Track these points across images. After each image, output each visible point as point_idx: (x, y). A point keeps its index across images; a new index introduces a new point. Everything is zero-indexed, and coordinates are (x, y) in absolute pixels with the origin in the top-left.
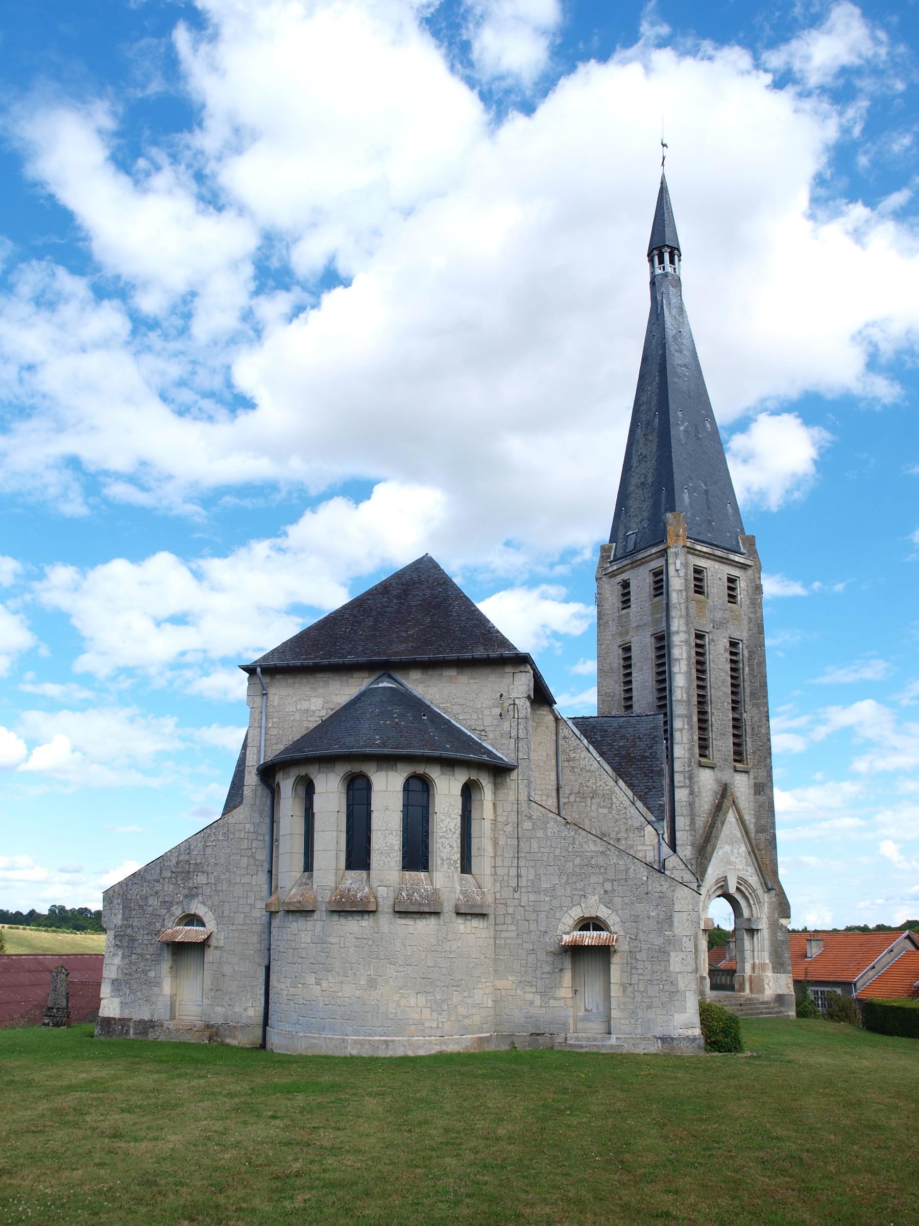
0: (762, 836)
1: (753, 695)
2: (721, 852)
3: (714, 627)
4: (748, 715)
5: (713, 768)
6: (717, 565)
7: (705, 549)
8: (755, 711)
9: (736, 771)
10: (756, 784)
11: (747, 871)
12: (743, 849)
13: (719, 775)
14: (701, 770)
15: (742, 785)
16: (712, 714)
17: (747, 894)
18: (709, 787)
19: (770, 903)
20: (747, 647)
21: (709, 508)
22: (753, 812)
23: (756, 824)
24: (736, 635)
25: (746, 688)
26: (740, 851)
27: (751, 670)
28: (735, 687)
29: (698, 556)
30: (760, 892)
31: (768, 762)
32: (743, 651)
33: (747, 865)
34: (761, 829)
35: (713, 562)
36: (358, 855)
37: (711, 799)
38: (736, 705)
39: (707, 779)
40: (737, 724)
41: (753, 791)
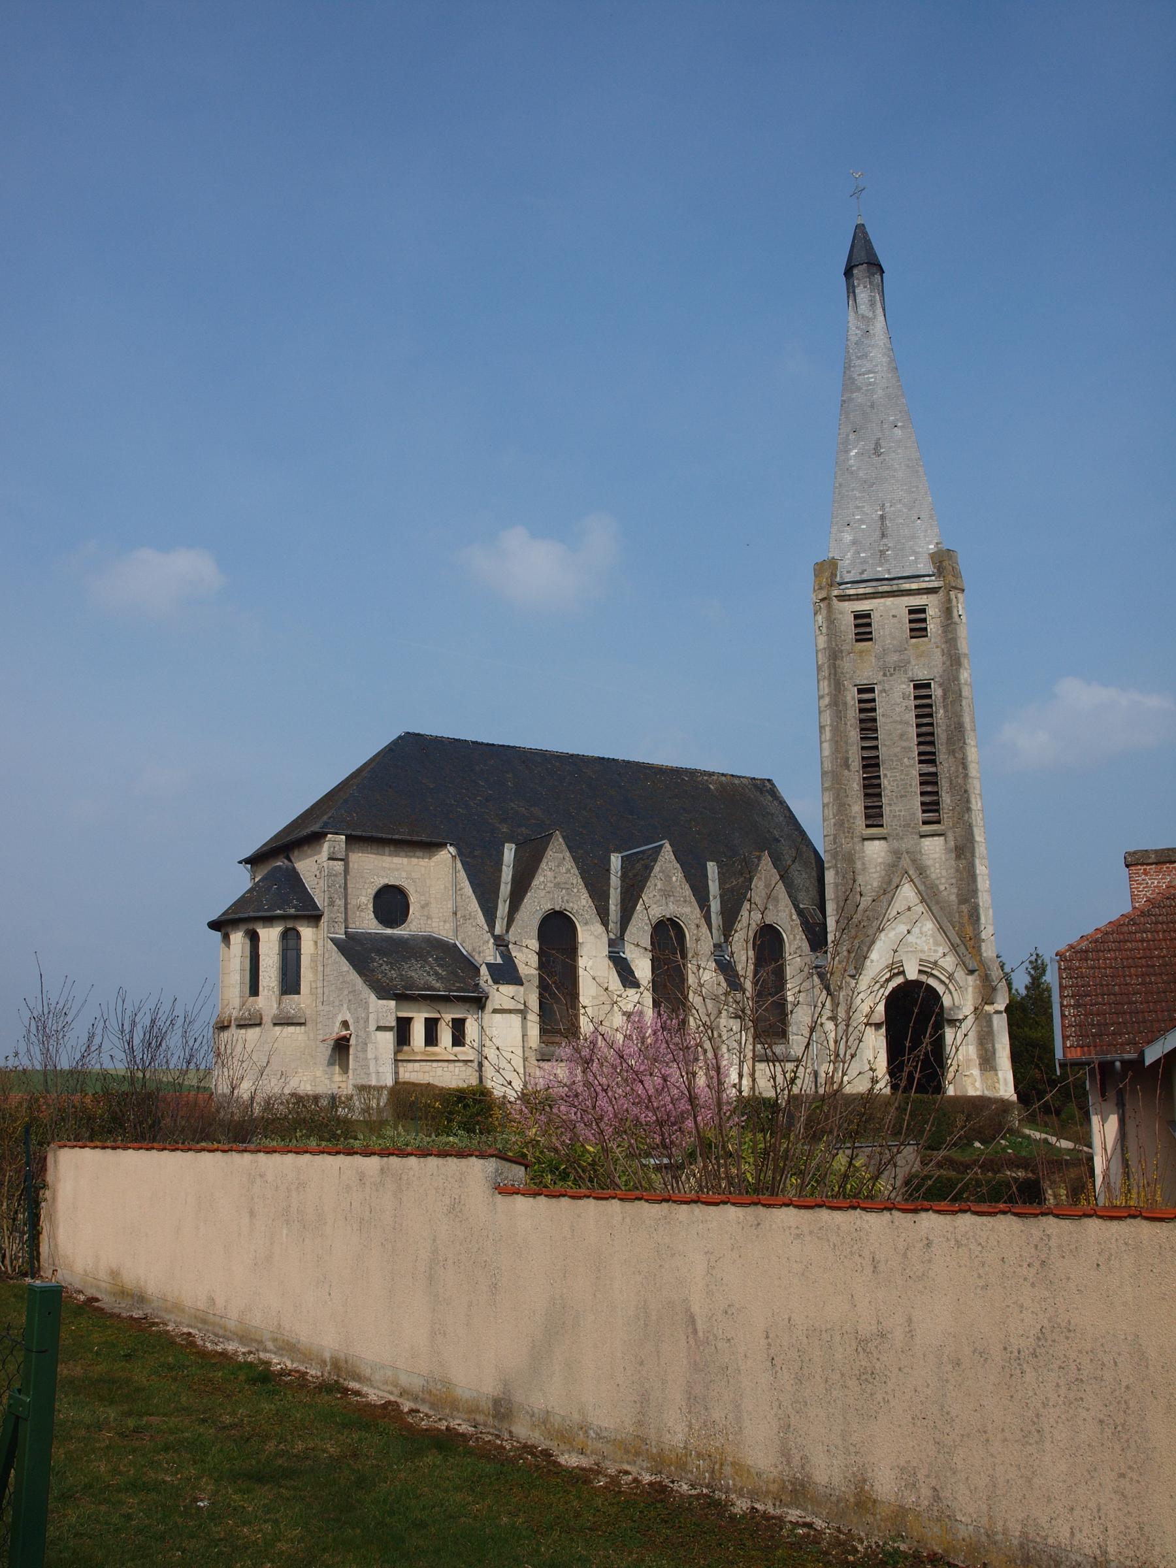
0: (965, 908)
1: (950, 741)
2: (892, 934)
3: (885, 675)
4: (945, 765)
5: (885, 839)
6: (889, 601)
7: (861, 591)
8: (951, 759)
9: (922, 836)
10: (956, 847)
11: (936, 951)
12: (929, 926)
13: (896, 844)
14: (866, 843)
15: (934, 850)
16: (885, 775)
17: (943, 978)
18: (880, 860)
19: (975, 987)
20: (941, 685)
21: (883, 536)
22: (954, 881)
23: (958, 895)
24: (922, 674)
25: (941, 734)
26: (925, 929)
27: (946, 711)
28: (926, 737)
29: (857, 600)
30: (960, 975)
31: (966, 817)
32: (937, 692)
33: (936, 944)
34: (963, 900)
35: (882, 600)
36: (254, 990)
37: (883, 873)
38: (927, 758)
39: (876, 851)
40: (929, 781)
41: (954, 855)
